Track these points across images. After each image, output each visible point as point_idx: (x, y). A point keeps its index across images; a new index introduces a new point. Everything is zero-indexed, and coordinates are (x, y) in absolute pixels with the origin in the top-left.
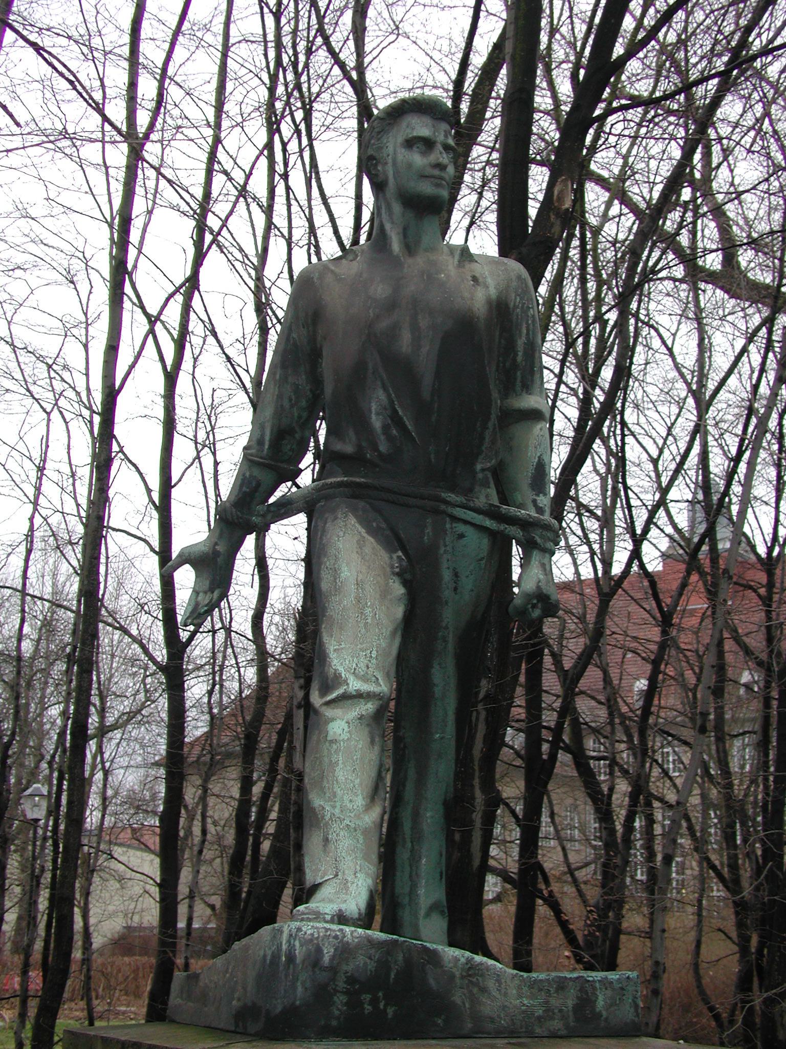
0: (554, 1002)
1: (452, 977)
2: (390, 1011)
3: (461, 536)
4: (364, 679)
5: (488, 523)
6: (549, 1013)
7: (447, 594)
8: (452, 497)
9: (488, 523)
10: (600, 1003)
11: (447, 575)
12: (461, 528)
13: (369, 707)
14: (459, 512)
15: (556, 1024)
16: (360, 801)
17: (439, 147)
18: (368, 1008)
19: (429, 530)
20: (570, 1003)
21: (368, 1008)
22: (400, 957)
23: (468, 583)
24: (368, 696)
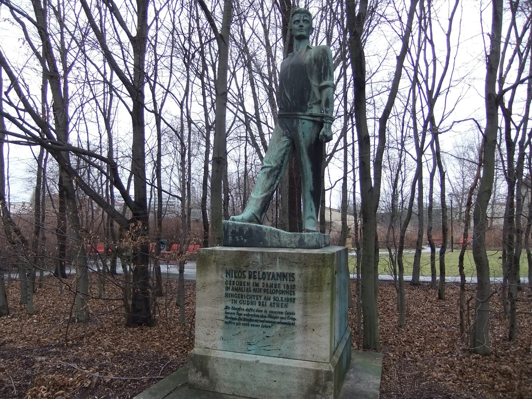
0: (293, 240)
1: (265, 233)
2: (245, 241)
3: (304, 123)
4: (268, 163)
5: (310, 118)
6: (291, 242)
7: (301, 138)
8: (300, 113)
9: (310, 118)
10: (306, 240)
11: (300, 134)
12: (303, 121)
13: (268, 169)
14: (302, 117)
15: (293, 245)
16: (260, 192)
17: (302, 21)
18: (238, 240)
19: (295, 123)
20: (297, 240)
21: (238, 240)
22: (247, 228)
23: (307, 135)
24: (268, 167)
